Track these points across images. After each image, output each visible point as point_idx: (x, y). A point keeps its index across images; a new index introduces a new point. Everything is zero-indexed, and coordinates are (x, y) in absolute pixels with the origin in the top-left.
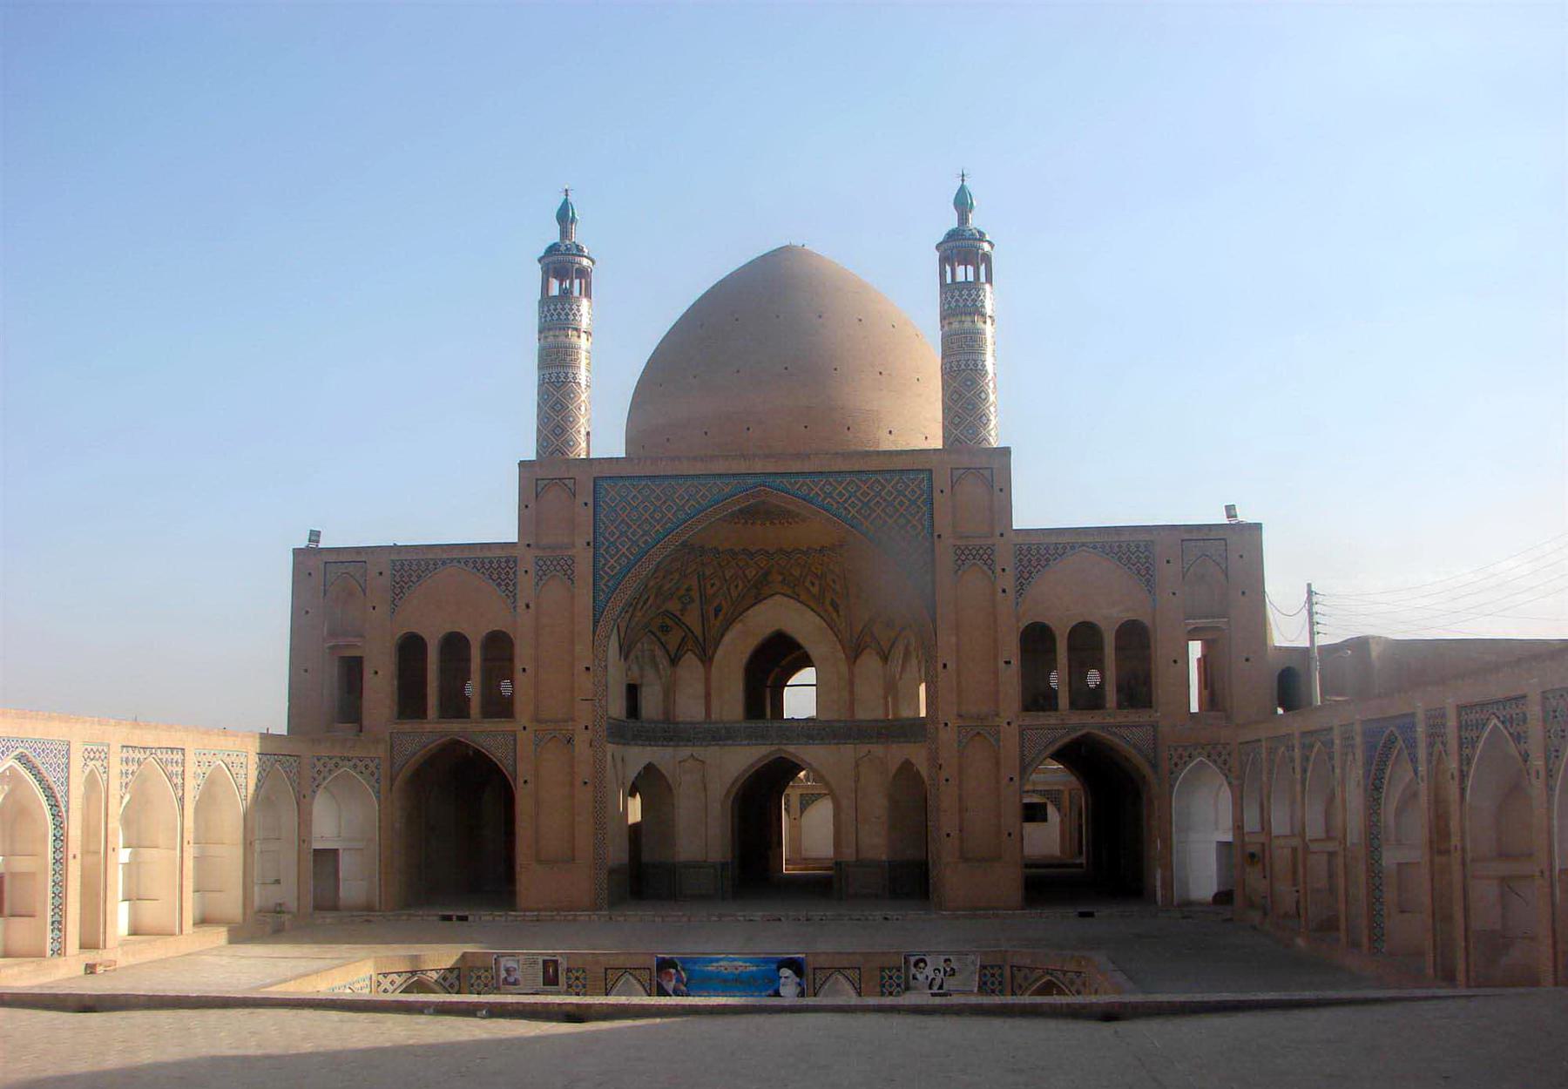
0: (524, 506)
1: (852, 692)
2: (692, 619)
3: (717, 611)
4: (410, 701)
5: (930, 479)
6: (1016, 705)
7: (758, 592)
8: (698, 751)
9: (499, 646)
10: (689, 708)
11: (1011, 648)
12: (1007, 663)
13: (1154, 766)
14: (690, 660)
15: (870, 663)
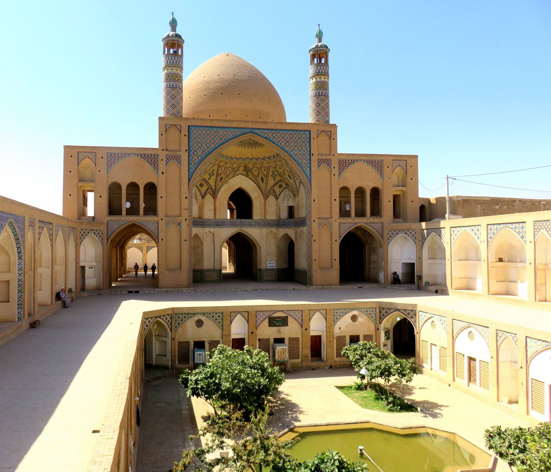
0: (161, 135)
1: (265, 210)
2: (212, 182)
3: (221, 179)
4: (114, 209)
5: (310, 134)
6: (338, 215)
7: (235, 173)
8: (212, 230)
9: (151, 188)
10: (208, 214)
11: (336, 195)
12: (335, 200)
13: (382, 237)
14: (209, 197)
15: (271, 199)
